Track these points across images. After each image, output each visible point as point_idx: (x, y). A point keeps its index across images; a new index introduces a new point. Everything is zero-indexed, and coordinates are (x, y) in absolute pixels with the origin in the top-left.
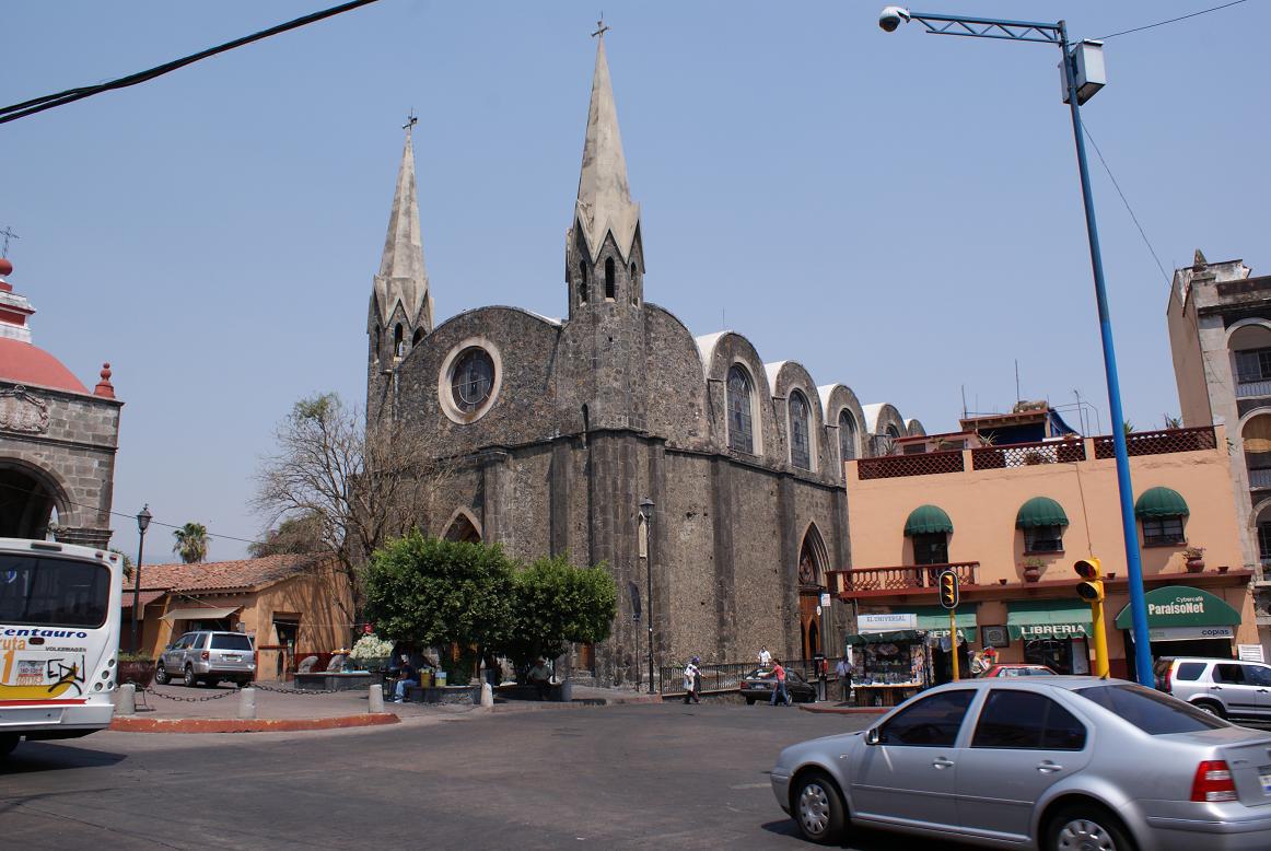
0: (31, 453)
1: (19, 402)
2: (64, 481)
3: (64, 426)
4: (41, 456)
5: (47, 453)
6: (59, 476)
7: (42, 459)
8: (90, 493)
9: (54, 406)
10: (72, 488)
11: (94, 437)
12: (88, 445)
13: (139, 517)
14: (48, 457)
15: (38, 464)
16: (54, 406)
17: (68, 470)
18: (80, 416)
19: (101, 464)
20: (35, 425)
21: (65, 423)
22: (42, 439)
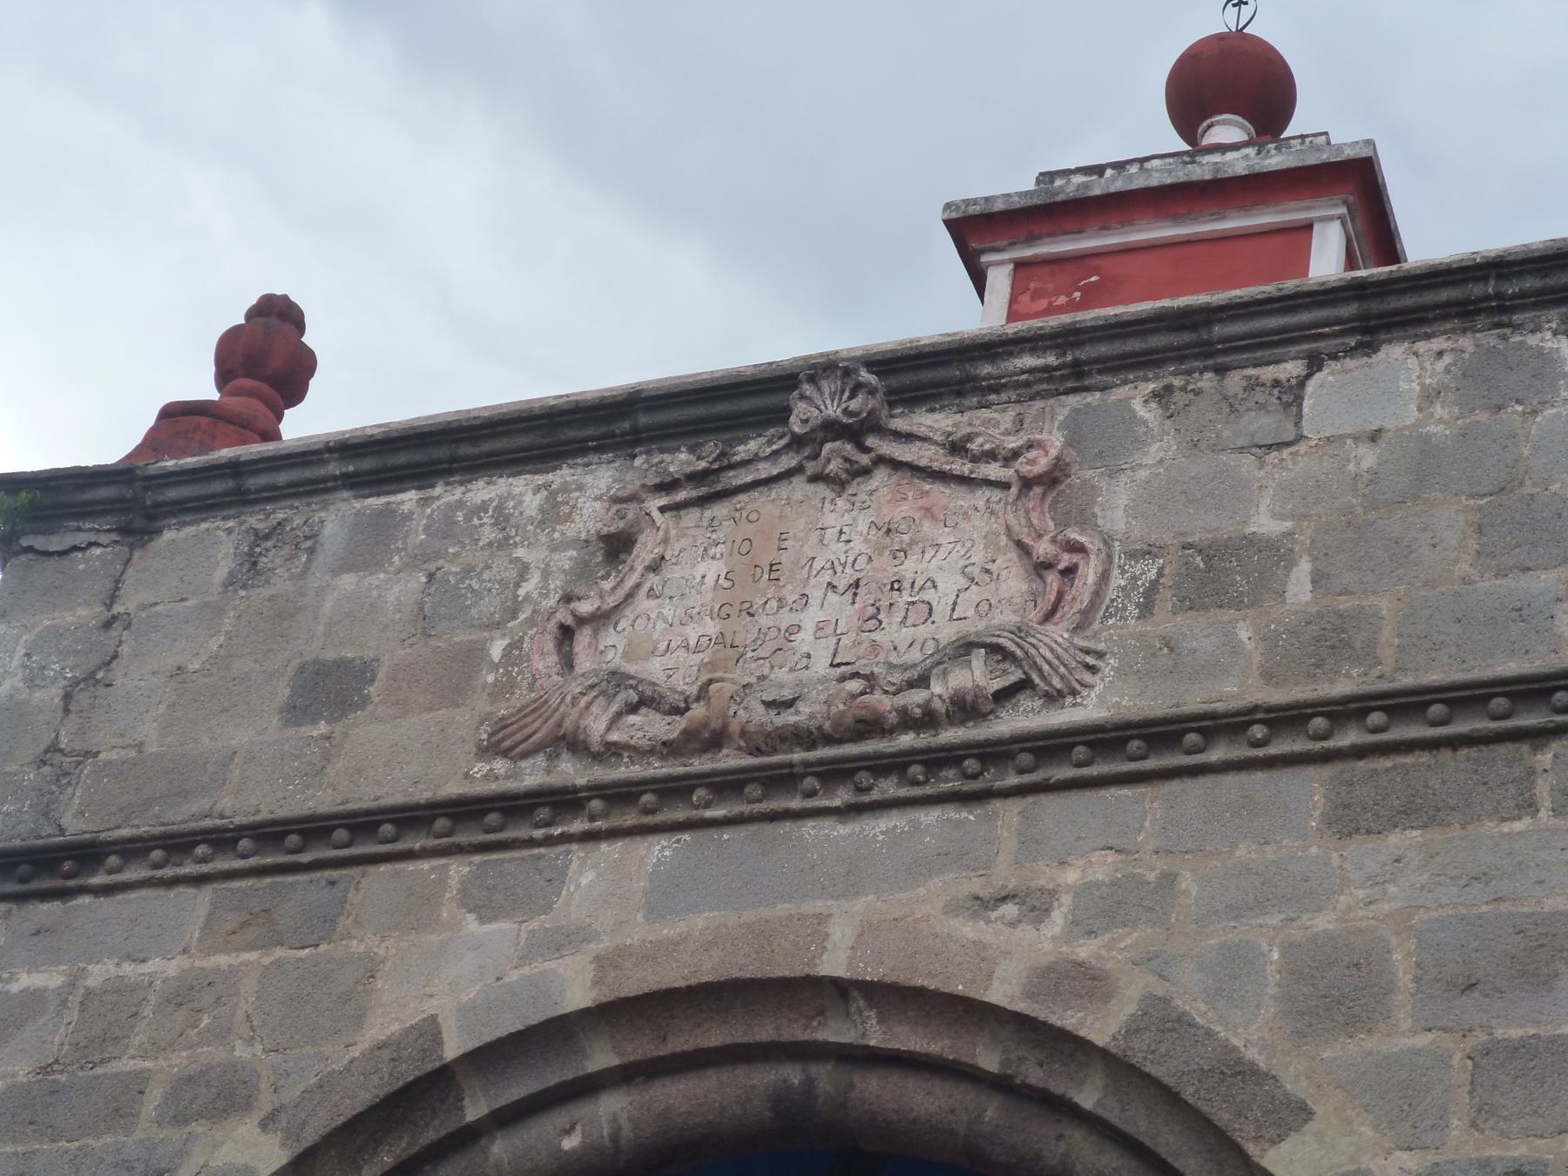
1: (836, 514)
4: (1036, 905)
5: (1101, 868)
6: (1238, 1071)
7: (1047, 939)
9: (1160, 451)
14: (1108, 908)
15: (1002, 992)
17: (1336, 991)
18: (1424, 465)
20: (965, 648)
21: (1277, 553)
22: (1052, 745)
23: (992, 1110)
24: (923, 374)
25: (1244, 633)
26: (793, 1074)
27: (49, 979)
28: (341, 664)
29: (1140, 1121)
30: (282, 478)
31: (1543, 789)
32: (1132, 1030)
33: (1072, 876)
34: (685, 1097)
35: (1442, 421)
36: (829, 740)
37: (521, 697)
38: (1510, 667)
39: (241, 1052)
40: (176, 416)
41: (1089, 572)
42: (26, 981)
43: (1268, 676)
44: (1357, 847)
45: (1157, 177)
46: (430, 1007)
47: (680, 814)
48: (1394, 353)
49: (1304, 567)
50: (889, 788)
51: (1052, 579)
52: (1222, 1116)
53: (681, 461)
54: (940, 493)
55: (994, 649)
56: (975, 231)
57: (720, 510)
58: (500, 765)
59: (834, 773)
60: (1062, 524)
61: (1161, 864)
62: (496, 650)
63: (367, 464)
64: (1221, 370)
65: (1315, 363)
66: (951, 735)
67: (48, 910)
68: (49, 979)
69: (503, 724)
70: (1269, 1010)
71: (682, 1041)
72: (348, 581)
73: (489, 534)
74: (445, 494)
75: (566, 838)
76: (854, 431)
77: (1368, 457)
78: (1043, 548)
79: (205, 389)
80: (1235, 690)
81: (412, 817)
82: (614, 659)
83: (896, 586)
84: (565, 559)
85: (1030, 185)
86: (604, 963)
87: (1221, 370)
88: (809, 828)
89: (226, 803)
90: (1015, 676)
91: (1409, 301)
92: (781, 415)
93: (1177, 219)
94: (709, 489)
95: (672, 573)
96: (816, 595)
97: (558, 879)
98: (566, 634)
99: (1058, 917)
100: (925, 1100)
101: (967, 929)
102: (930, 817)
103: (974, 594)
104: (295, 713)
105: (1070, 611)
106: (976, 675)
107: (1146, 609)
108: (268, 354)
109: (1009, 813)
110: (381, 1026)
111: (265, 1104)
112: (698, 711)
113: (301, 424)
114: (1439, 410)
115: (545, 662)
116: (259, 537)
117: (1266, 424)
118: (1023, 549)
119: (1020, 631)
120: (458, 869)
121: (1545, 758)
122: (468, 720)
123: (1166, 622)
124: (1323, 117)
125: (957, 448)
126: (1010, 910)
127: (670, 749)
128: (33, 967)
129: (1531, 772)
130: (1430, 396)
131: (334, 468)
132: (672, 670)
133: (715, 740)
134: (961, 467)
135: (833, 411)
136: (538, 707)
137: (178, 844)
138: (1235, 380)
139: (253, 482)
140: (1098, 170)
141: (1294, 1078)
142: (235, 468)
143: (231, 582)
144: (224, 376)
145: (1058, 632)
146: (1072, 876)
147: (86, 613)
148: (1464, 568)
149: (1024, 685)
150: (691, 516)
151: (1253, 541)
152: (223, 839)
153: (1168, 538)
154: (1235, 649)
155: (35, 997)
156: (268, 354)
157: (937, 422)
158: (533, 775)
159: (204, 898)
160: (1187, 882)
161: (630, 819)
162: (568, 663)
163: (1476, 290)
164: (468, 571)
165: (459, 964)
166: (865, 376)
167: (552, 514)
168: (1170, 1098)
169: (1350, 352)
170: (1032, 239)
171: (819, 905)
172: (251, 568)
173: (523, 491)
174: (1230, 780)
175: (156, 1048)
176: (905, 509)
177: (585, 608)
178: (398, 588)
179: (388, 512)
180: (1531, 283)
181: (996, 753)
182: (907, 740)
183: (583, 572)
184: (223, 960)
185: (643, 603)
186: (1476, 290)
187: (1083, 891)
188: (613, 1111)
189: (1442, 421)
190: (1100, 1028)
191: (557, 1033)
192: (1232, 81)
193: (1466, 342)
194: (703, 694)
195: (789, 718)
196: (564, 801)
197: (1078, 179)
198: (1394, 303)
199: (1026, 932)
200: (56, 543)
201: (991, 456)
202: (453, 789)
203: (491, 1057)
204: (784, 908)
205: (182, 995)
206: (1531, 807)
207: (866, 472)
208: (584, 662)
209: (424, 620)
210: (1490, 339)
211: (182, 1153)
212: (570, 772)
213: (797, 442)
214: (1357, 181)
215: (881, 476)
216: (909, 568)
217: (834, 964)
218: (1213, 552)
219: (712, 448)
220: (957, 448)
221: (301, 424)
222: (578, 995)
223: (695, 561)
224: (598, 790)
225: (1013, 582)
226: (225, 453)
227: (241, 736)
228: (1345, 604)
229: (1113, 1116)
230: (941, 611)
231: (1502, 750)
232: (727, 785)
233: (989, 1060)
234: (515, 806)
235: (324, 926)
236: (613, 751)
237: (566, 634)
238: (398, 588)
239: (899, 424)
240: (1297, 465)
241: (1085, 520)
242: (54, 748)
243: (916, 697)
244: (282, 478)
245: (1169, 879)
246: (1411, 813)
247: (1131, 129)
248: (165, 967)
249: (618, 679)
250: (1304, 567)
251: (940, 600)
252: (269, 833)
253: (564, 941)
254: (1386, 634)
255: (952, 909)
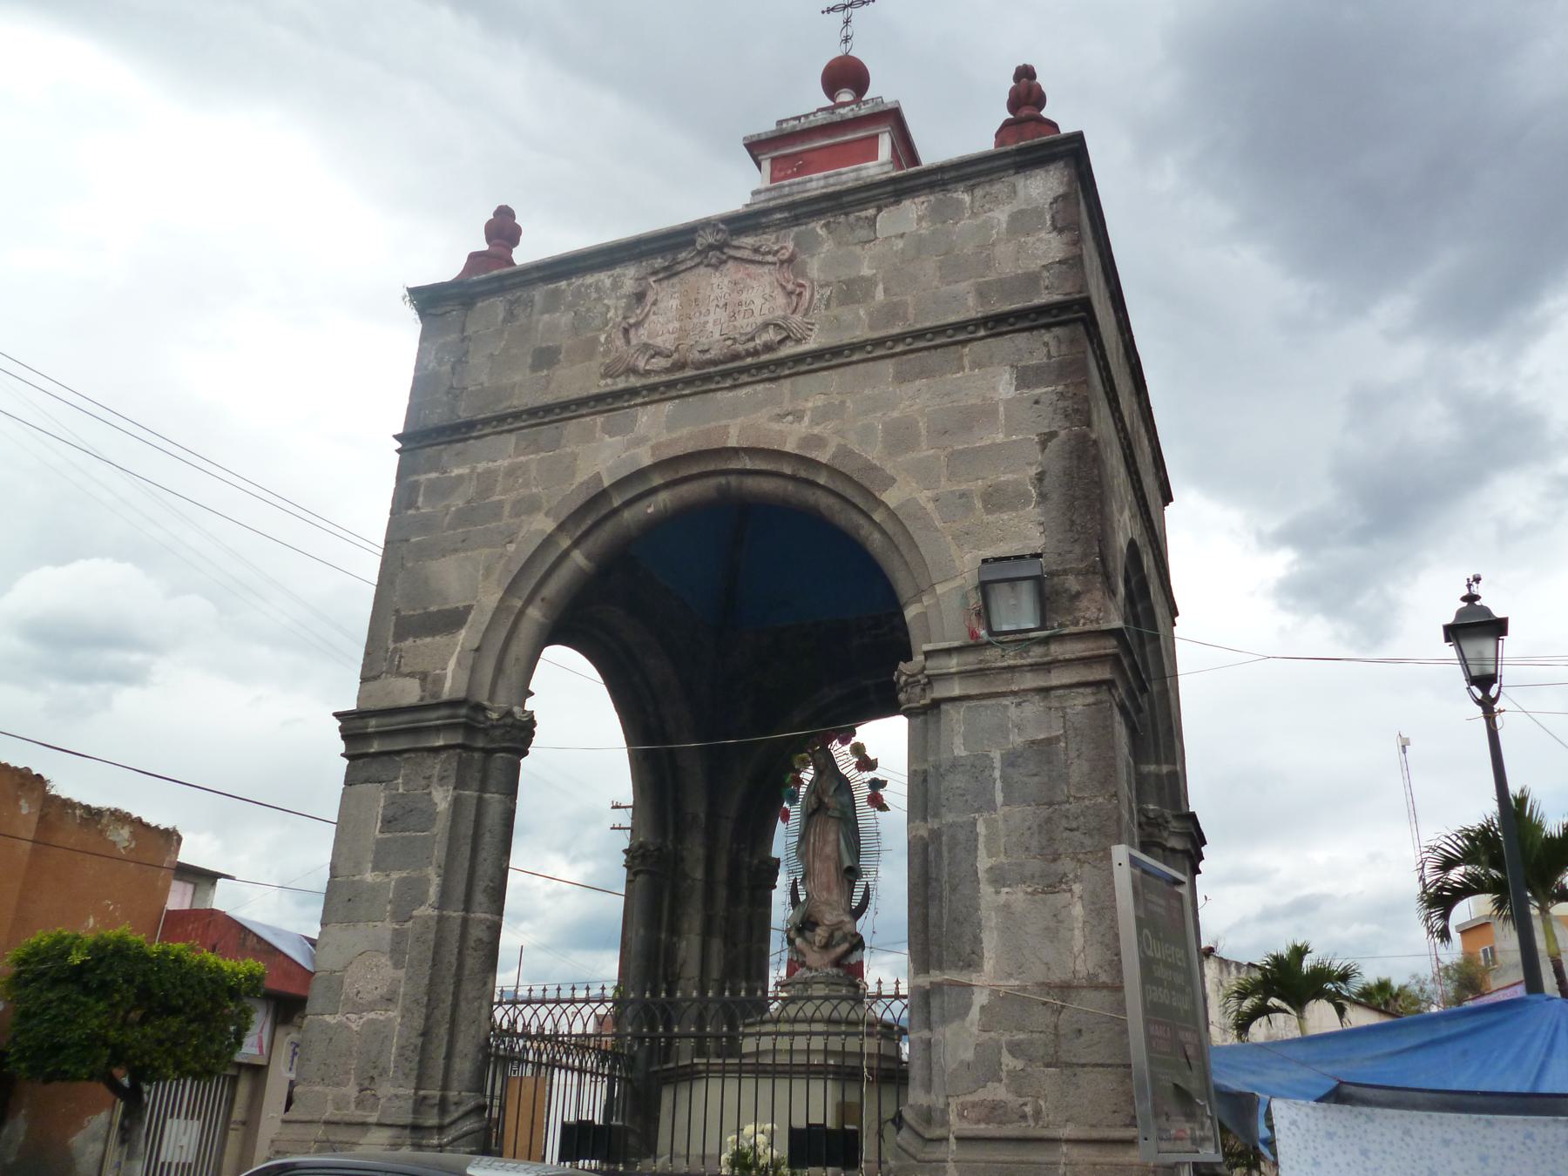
0: (762, 418)
1: (716, 279)
2: (890, 481)
3: (869, 294)
4: (798, 416)
5: (819, 401)
7: (803, 427)
8: (996, 499)
9: (828, 246)
10: (923, 497)
11: (982, 293)
12: (960, 327)
13: (1453, 633)
14: (822, 415)
16: (828, 246)
17: (901, 437)
18: (920, 245)
19: (1025, 378)
20: (766, 325)
21: (870, 282)
22: (799, 359)
23: (790, 487)
24: (740, 224)
25: (862, 312)
26: (722, 480)
27: (464, 470)
28: (549, 348)
29: (839, 487)
30: (517, 280)
31: (966, 361)
32: (834, 457)
33: (810, 405)
34: (688, 491)
35: (925, 228)
36: (722, 362)
37: (613, 355)
38: (952, 319)
39: (534, 490)
40: (473, 257)
41: (807, 294)
42: (456, 472)
43: (871, 328)
44: (905, 387)
45: (822, 118)
46: (597, 469)
47: (674, 393)
48: (907, 203)
49: (881, 287)
50: (745, 378)
51: (794, 298)
52: (867, 484)
53: (659, 262)
54: (752, 268)
55: (776, 325)
56: (756, 147)
57: (675, 280)
58: (609, 381)
59: (725, 374)
60: (796, 277)
61: (840, 398)
62: (602, 339)
63: (547, 272)
64: (847, 214)
65: (879, 210)
66: (764, 358)
67: (459, 446)
68: (464, 470)
69: (608, 367)
70: (880, 446)
71: (684, 473)
72: (546, 317)
73: (594, 295)
74: (577, 282)
75: (636, 405)
76: (720, 247)
77: (900, 244)
78: (790, 287)
79: (483, 246)
80: (862, 333)
81: (581, 402)
82: (644, 339)
83: (740, 304)
84: (623, 303)
85: (773, 127)
86: (654, 448)
87: (847, 214)
88: (719, 394)
89: (516, 402)
90: (785, 334)
91: (911, 183)
92: (693, 242)
93: (830, 137)
94: (670, 273)
95: (662, 305)
96: (712, 310)
97: (634, 420)
98: (626, 331)
99: (806, 420)
100: (767, 485)
101: (776, 426)
102: (760, 387)
103: (767, 305)
104: (535, 367)
105: (801, 309)
106: (771, 336)
107: (827, 306)
108: (503, 229)
109: (787, 383)
110: (581, 477)
111: (546, 506)
112: (676, 356)
113: (523, 255)
114: (924, 224)
115: (620, 342)
116: (511, 303)
117: (863, 233)
118: (784, 288)
119: (785, 318)
120: (600, 419)
121: (966, 350)
122: (596, 365)
123: (836, 310)
124: (881, 90)
125: (756, 250)
126: (790, 418)
127: (667, 370)
128: (458, 466)
129: (961, 357)
130: (920, 219)
131: (535, 275)
132: (664, 341)
133: (681, 366)
134: (758, 258)
135: (711, 240)
136: (619, 359)
137: (501, 419)
138: (852, 217)
139: (508, 282)
140: (798, 118)
141: (889, 469)
142: (499, 278)
143: (505, 321)
144: (489, 240)
145: (798, 317)
146: (810, 405)
147: (453, 337)
148: (935, 283)
149: (788, 337)
150: (665, 283)
151: (863, 278)
152: (516, 416)
153: (832, 279)
154: (859, 318)
155: (460, 478)
156: (503, 229)
157: (748, 241)
158: (621, 384)
159: (513, 438)
160: (849, 403)
161: (656, 396)
162: (628, 342)
163: (934, 178)
164: (588, 310)
165: (606, 453)
166: (722, 226)
167: (616, 285)
168: (848, 478)
169: (892, 204)
170: (776, 149)
171: (723, 422)
172: (511, 316)
173: (605, 278)
174: (861, 366)
175: (505, 491)
176: (740, 275)
177: (632, 321)
178: (564, 319)
179: (557, 290)
180: (953, 174)
181: (780, 363)
182: (749, 360)
183: (629, 308)
184: (522, 458)
185: (652, 317)
186: (934, 178)
187: (816, 408)
188: (664, 499)
189: (925, 228)
190: (823, 457)
191: (641, 474)
192: (846, 75)
193: (932, 198)
194: (677, 349)
195: (708, 356)
196: (633, 392)
197: (792, 123)
198: (906, 185)
199: (796, 425)
200: (440, 311)
201: (769, 253)
202: (594, 391)
203: (620, 484)
204: (713, 424)
205: (511, 472)
206: (962, 368)
207: (725, 262)
208: (634, 342)
209: (575, 330)
210: (940, 195)
211: (520, 527)
212: (634, 381)
213: (699, 253)
214: (893, 117)
215: (730, 264)
216: (744, 297)
217: (732, 443)
218: (850, 283)
219: (669, 257)
220: (756, 250)
221: (523, 255)
222: (647, 460)
223: (668, 301)
224: (644, 387)
225: (781, 300)
226: (495, 272)
227: (517, 378)
228: (895, 299)
229: (831, 485)
230: (757, 312)
231: (952, 348)
232: (689, 382)
233: (788, 470)
234: (617, 395)
235: (556, 444)
236: (648, 373)
237: (626, 331)
238: (564, 319)
239: (735, 243)
240: (876, 248)
241: (804, 275)
242: (452, 387)
243: (751, 345)
244: (517, 280)
245: (843, 403)
246: (923, 373)
247: (811, 100)
248: (503, 463)
249: (646, 346)
250: (881, 287)
251: (756, 308)
252: (533, 412)
253: (639, 442)
254: (911, 310)
255: (771, 419)
